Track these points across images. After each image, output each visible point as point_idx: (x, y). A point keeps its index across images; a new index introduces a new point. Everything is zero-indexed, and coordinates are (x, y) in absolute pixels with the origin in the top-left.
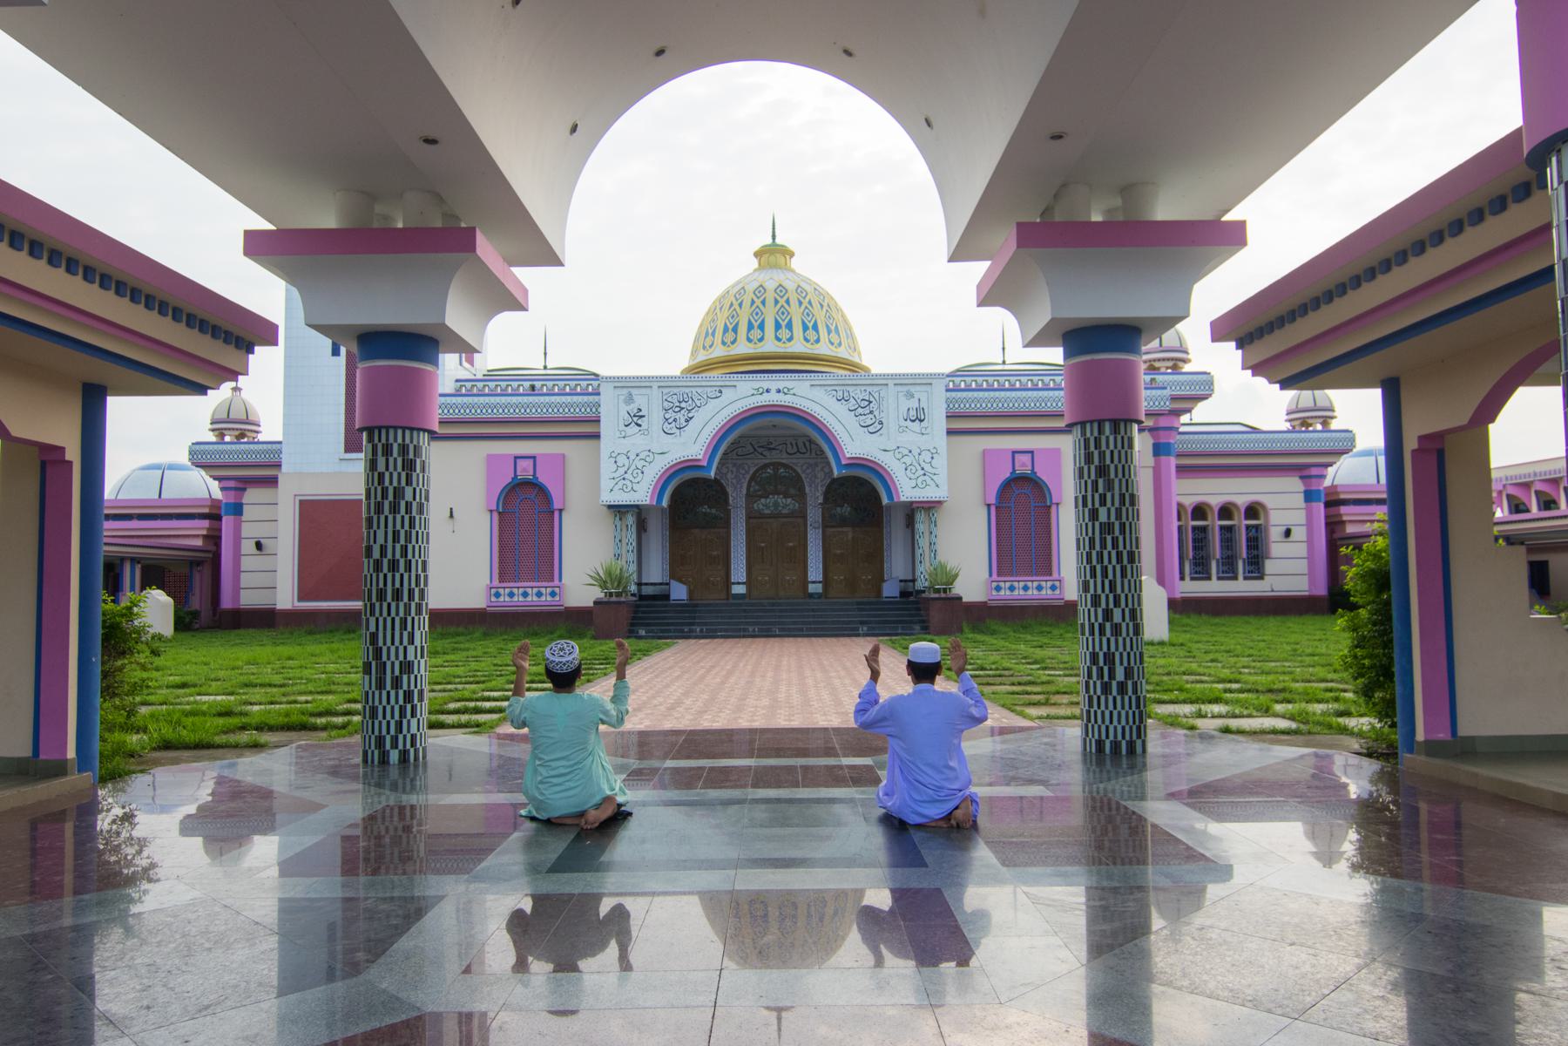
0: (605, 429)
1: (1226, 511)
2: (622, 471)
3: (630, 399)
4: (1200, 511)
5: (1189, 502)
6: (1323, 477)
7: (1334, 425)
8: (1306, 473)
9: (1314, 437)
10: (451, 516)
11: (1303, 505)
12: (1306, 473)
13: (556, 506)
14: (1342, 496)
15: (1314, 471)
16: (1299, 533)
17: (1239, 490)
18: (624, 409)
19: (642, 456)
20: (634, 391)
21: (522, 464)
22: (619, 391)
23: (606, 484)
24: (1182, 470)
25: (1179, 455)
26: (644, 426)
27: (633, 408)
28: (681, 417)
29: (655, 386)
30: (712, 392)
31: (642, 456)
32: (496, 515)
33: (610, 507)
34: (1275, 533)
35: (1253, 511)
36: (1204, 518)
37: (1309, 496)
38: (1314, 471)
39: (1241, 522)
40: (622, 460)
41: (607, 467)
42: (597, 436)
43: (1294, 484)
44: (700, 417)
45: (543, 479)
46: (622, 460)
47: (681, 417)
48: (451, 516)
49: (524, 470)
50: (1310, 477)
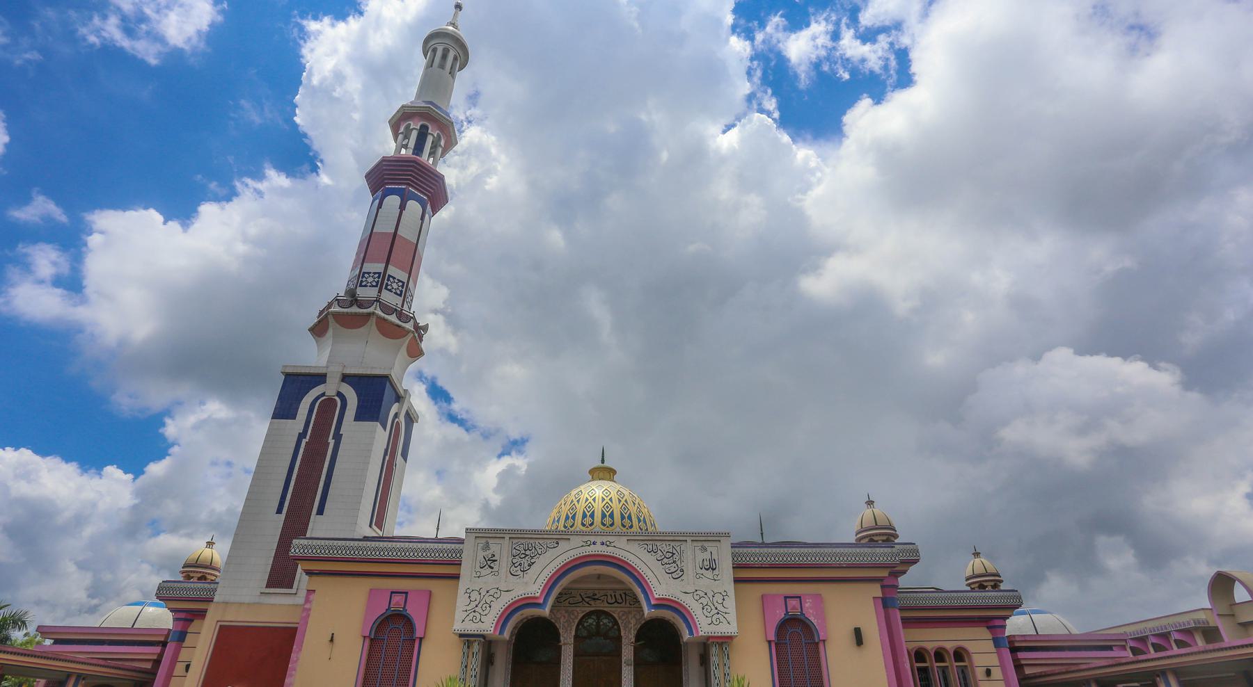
0: (465, 571)
1: (939, 655)
2: (473, 604)
3: (487, 547)
4: (919, 655)
5: (913, 646)
6: (1004, 627)
7: (1002, 587)
8: (991, 624)
9: (989, 597)
10: (332, 640)
11: (994, 650)
12: (991, 624)
13: (418, 634)
14: (1017, 645)
15: (997, 623)
16: (997, 673)
17: (947, 638)
18: (481, 554)
19: (491, 592)
20: (491, 541)
21: (396, 598)
22: (478, 541)
23: (459, 615)
24: (907, 622)
25: (902, 609)
26: (496, 568)
27: (488, 553)
28: (525, 562)
29: (507, 537)
30: (551, 543)
31: (491, 592)
32: (368, 641)
33: (461, 636)
34: (980, 673)
35: (959, 655)
36: (925, 661)
37: (997, 642)
38: (997, 623)
39: (952, 665)
40: (475, 595)
41: (462, 601)
42: (456, 577)
43: (983, 632)
44: (540, 562)
45: (410, 611)
46: (475, 595)
47: (525, 562)
48: (332, 640)
49: (398, 603)
50: (995, 627)
